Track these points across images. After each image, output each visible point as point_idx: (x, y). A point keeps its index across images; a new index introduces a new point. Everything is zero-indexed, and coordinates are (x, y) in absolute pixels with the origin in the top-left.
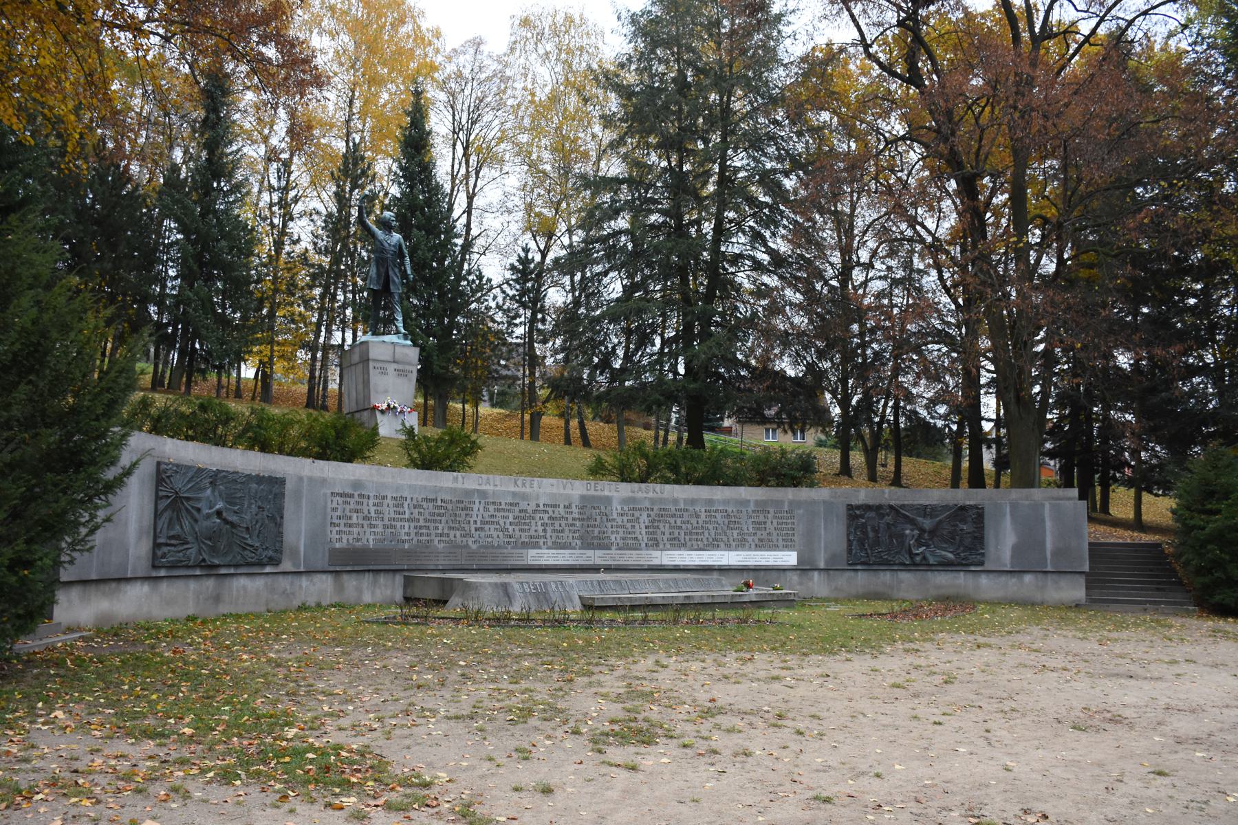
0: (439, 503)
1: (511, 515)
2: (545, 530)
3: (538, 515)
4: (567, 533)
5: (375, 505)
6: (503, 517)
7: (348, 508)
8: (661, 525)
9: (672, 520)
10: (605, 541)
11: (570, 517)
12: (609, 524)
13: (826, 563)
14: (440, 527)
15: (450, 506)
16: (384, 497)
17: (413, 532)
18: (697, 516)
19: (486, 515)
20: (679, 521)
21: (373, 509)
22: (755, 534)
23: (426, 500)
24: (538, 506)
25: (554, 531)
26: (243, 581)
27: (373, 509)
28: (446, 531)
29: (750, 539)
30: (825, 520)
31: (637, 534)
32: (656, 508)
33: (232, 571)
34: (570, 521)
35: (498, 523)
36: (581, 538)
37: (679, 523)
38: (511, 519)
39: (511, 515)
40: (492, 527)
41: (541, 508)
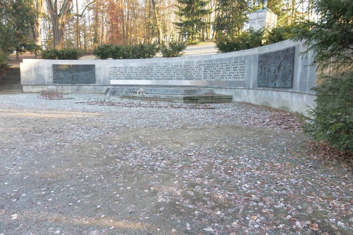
0: (143, 68)
1: (164, 70)
2: (174, 74)
3: (172, 69)
4: (181, 75)
5: (124, 69)
6: (162, 71)
7: (116, 70)
8: (208, 70)
9: (210, 68)
10: (192, 77)
11: (182, 69)
12: (193, 71)
13: (252, 87)
14: (144, 74)
15: (146, 68)
16: (127, 67)
17: (136, 76)
18: (218, 66)
19: (157, 70)
20: (213, 68)
21: (123, 70)
22: (234, 73)
23: (139, 67)
24: (172, 66)
25: (177, 74)
26: (86, 87)
27: (123, 70)
28: (145, 75)
29: (232, 74)
30: (253, 64)
31: (201, 75)
32: (206, 64)
33: (80, 84)
34: (182, 71)
35: (160, 72)
36: (185, 76)
37: (213, 70)
38: (165, 71)
39: (164, 70)
40: (159, 74)
41: (173, 67)
